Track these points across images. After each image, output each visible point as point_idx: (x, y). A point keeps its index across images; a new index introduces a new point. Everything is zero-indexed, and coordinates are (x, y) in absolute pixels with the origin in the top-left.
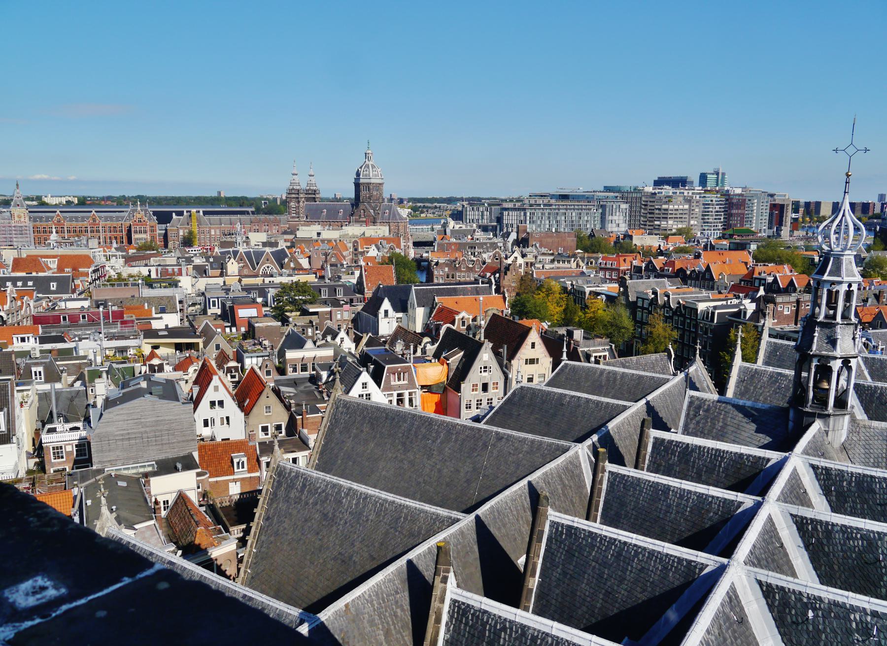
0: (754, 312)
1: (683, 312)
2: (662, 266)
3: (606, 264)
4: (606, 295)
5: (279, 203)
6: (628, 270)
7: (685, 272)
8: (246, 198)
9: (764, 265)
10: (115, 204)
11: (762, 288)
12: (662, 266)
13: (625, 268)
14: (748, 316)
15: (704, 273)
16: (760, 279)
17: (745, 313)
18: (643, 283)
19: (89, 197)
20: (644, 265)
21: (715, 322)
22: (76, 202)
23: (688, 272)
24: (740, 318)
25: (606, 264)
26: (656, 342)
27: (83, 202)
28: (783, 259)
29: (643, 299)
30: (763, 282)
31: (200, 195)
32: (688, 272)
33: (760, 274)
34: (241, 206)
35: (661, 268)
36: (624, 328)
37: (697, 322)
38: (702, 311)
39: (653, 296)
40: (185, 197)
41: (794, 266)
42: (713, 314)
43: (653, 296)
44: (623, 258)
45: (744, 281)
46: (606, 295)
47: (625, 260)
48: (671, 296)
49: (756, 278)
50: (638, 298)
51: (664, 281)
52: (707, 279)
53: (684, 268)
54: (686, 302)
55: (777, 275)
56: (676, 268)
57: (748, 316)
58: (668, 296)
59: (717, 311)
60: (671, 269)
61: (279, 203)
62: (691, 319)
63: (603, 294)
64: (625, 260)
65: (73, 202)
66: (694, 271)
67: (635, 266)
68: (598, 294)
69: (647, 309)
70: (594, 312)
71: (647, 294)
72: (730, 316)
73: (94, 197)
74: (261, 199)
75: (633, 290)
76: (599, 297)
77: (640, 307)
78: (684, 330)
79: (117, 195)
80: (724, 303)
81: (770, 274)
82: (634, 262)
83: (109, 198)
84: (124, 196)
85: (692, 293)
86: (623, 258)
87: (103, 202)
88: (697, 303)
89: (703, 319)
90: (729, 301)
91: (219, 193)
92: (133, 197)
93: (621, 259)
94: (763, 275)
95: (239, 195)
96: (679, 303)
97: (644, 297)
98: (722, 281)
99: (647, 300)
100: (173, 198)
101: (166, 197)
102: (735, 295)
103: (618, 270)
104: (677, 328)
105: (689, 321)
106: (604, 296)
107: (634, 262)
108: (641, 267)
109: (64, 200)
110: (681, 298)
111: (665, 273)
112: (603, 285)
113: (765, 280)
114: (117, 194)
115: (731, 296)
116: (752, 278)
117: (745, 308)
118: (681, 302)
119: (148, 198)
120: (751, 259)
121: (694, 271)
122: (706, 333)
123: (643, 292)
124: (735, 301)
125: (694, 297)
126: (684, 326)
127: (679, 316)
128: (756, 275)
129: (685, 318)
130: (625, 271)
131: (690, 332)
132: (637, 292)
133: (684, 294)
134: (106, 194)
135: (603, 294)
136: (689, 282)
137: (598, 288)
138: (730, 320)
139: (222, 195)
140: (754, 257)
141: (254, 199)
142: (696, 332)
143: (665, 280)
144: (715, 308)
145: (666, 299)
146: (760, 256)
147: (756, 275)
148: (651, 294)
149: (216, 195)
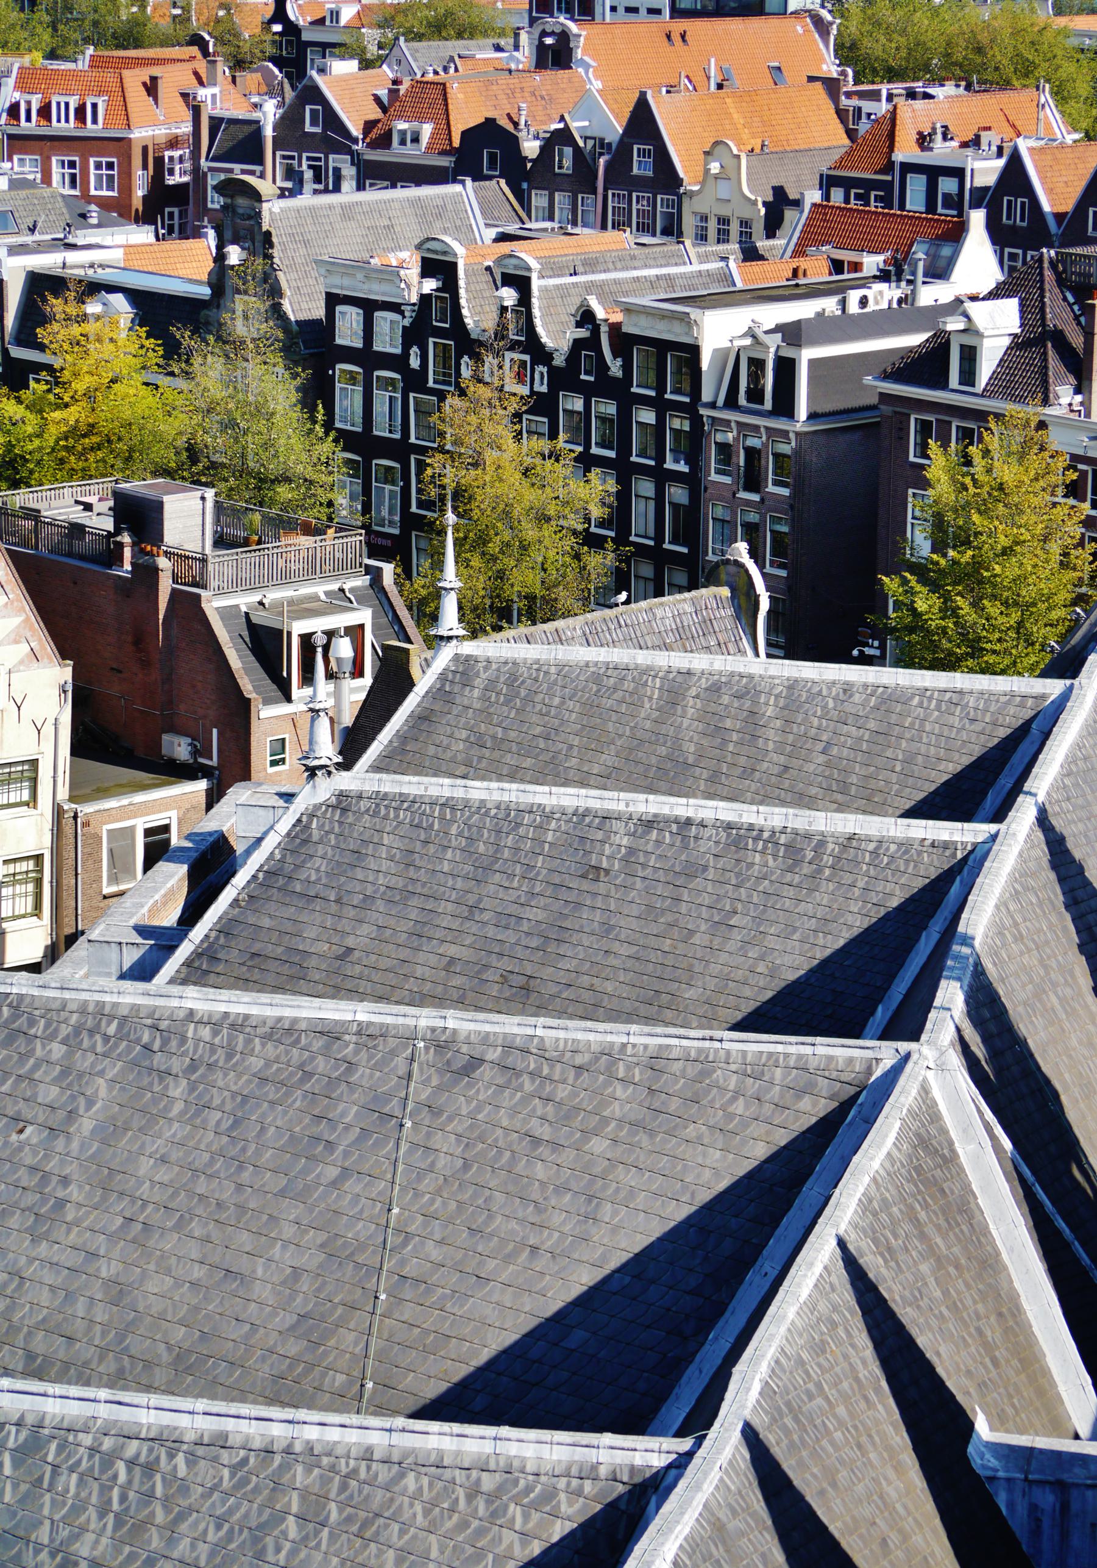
0: (1018, 344)
1: (615, 367)
2: (375, 113)
3: (45, 112)
4: (136, 296)
6: (174, 143)
7: (511, 142)
9: (911, 95)
11: (977, 218)
12: (375, 113)
13: (161, 132)
14: (986, 369)
15: (621, 155)
16: (933, 173)
17: (970, 355)
18: (347, 212)
20: (270, 113)
21: (802, 410)
23: (531, 148)
24: (941, 382)
25: (45, 112)
26: (493, 548)
28: (1000, 56)
29: (369, 307)
30: (947, 185)
32: (531, 148)
33: (924, 141)
35: (369, 126)
36: (288, 480)
37: (697, 421)
38: (721, 355)
39: (430, 285)
41: (1061, 95)
42: (786, 368)
43: (430, 285)
44: (144, 74)
45: (847, 184)
46: (136, 296)
47: (152, 88)
48: (536, 284)
49: (908, 168)
50: (333, 300)
51: (456, 198)
52: (640, 183)
53: (504, 123)
54: (628, 310)
55: (1024, 145)
56: (458, 128)
57: (986, 369)
58: (521, 284)
59: (807, 355)
60: (427, 130)
62: (661, 406)
63: (112, 289)
64: (152, 88)
66: (563, 136)
67: (216, 123)
68: (93, 288)
69: (398, 362)
70: (90, 395)
71: (392, 274)
72: (886, 376)
75: (300, 254)
76: (93, 308)
77: (348, 354)
78: (624, 470)
80: (829, 305)
81: (976, 142)
82: (204, 93)
85: (625, 261)
86: (144, 74)
88: (694, 313)
89: (731, 402)
90: (854, 296)
93: (135, 79)
94: (938, 142)
96: (586, 317)
97: (376, 292)
98: (723, 190)
99: (395, 308)
102: (837, 266)
103: (121, 145)
104: (586, 462)
105: (648, 416)
106: (119, 301)
107: (204, 93)
108: (256, 128)
110: (589, 288)
111: (399, 153)
112: (81, 237)
113: (958, 173)
115: (817, 270)
116: (889, 167)
117: (970, 330)
118: (600, 313)
120: (830, 67)
121: (563, 136)
122: (753, 482)
123: (362, 266)
124: (883, 295)
125: (653, 283)
126: (624, 449)
127: (587, 392)
128: (906, 151)
129: (627, 402)
130: (158, 148)
131: (661, 477)
132: (331, 267)
133: (592, 264)
135: (112, 289)
136: (539, 199)
137: (73, 257)
138: (884, 397)
140: (847, 52)
142: (693, 481)
143: (465, 191)
144: (793, 333)
145: (509, 296)
146: (877, 46)
147: (906, 151)
148: (413, 273)
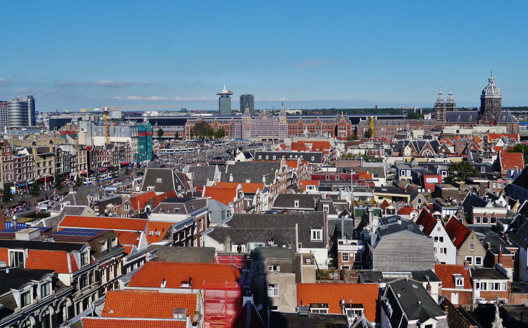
5: (415, 111)
8: (393, 109)
10: (321, 113)
19: (306, 110)
22: (301, 112)
27: (305, 112)
31: (367, 108)
34: (393, 114)
40: (358, 109)
61: (415, 111)
65: (299, 113)
73: (309, 110)
74: (402, 109)
79: (321, 109)
83: (317, 110)
84: (324, 109)
87: (314, 113)
91: (377, 106)
92: (329, 109)
95: (389, 107)
100: (351, 110)
101: (347, 109)
109: (295, 112)
114: (320, 108)
119: (337, 110)
134: (315, 108)
139: (378, 108)
141: (398, 110)
149: (374, 107)
